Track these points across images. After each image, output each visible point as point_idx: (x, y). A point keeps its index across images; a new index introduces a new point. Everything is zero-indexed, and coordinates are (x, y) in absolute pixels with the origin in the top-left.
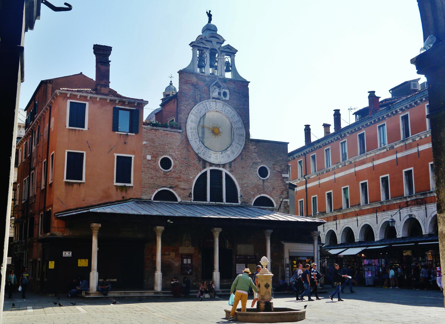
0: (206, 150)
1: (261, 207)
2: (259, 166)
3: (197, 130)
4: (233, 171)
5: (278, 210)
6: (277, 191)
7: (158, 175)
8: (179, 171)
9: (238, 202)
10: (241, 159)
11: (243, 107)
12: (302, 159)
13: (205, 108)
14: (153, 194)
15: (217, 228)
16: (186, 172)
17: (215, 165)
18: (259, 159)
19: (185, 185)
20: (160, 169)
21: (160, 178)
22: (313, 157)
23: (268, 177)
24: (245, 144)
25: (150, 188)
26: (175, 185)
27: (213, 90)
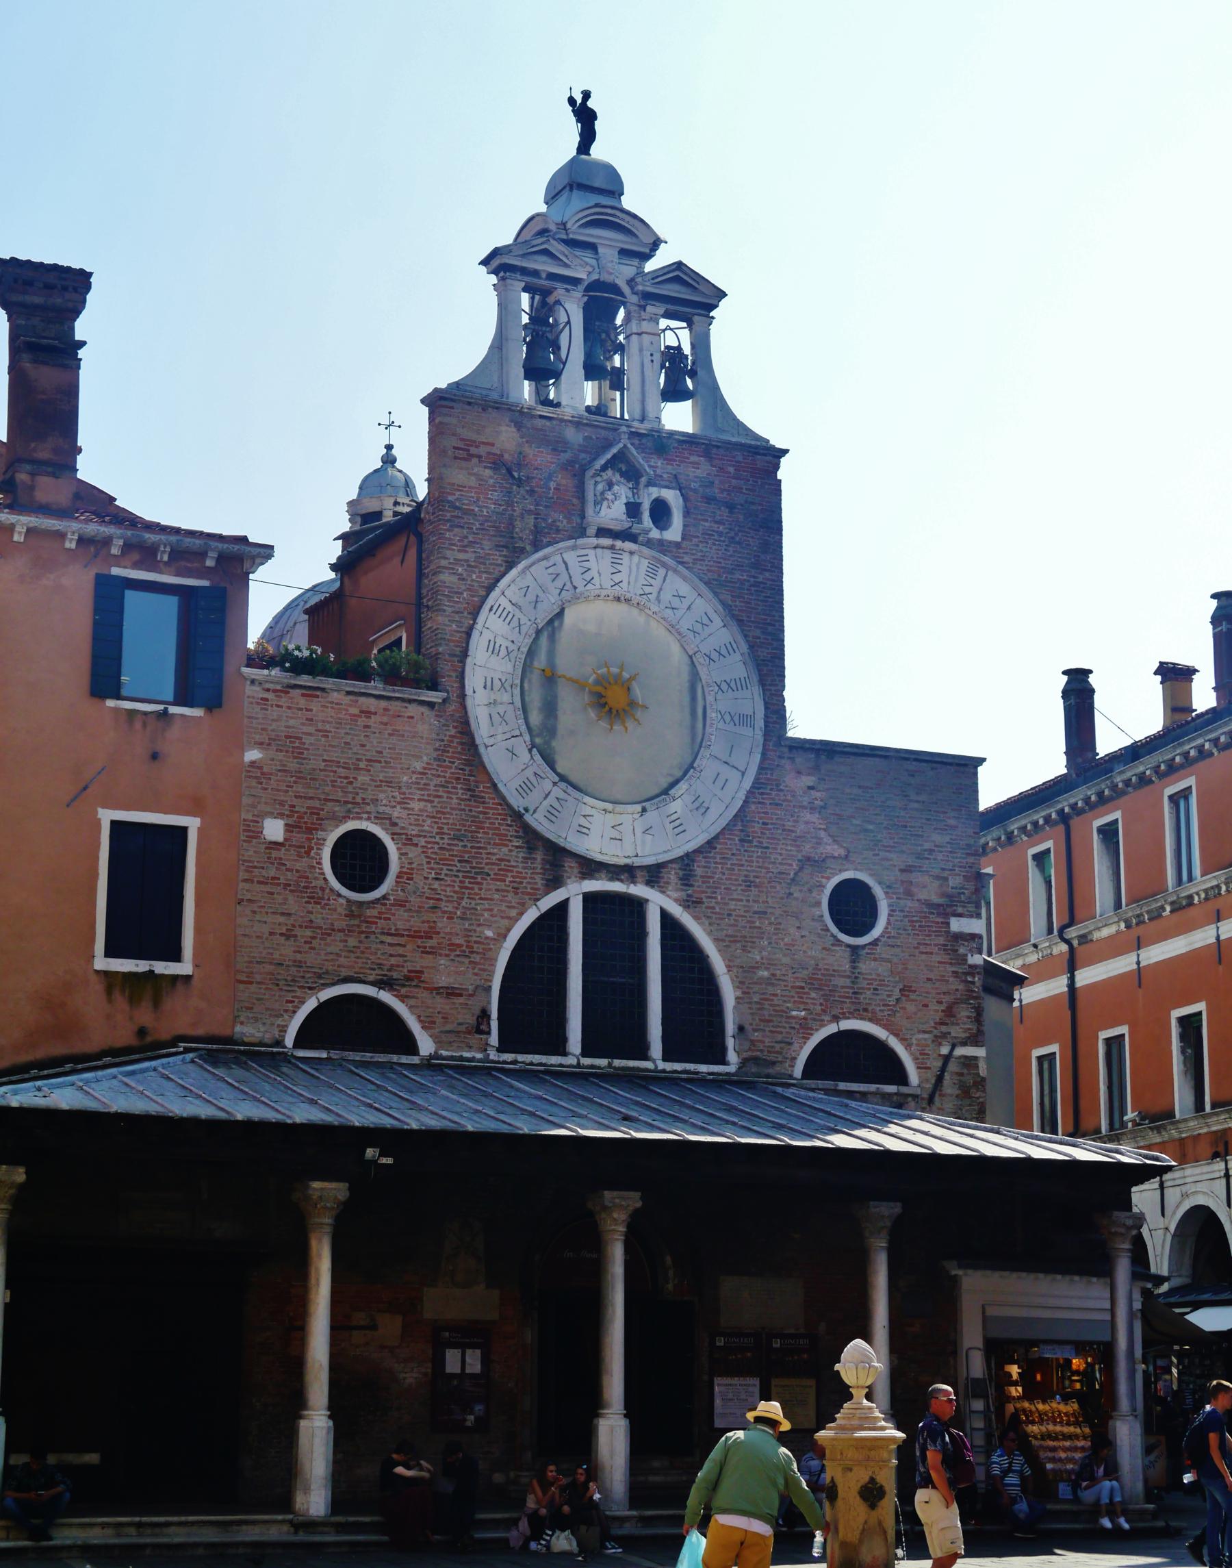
0: (562, 795)
1: (842, 1086)
2: (835, 874)
3: (519, 688)
4: (699, 902)
5: (931, 1100)
6: (926, 1006)
7: (318, 920)
9: (723, 1061)
10: (741, 840)
11: (752, 579)
12: (1049, 844)
13: (559, 583)
14: (292, 1017)
15: (615, 1193)
16: (464, 903)
17: (608, 872)
19: (458, 973)
20: (332, 890)
21: (329, 935)
22: (1109, 833)
23: (876, 932)
25: (278, 985)
26: (405, 970)
27: (602, 493)
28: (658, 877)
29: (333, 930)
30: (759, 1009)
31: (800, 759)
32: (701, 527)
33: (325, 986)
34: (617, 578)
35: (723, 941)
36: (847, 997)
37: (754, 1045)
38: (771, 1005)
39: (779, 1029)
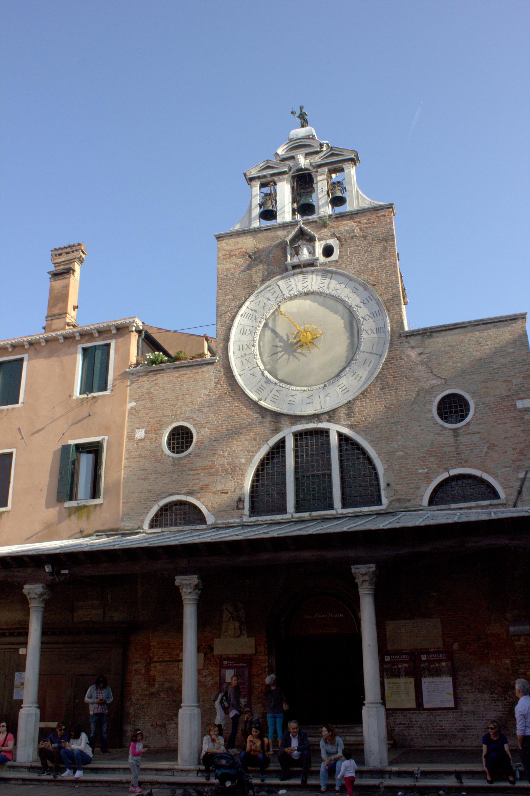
0: (280, 389)
1: (453, 506)
2: (439, 394)
6: (506, 452)
8: (210, 450)
10: (380, 389)
13: (276, 295)
14: (146, 515)
15: (182, 577)
18: (435, 377)
20: (165, 455)
21: (164, 475)
23: (468, 419)
24: (390, 348)
25: (140, 502)
28: (333, 417)
29: (166, 473)
30: (399, 473)
31: (413, 341)
32: (348, 250)
33: (162, 498)
34: (305, 285)
35: (374, 441)
36: (453, 457)
37: (397, 492)
38: (406, 469)
39: (412, 481)
